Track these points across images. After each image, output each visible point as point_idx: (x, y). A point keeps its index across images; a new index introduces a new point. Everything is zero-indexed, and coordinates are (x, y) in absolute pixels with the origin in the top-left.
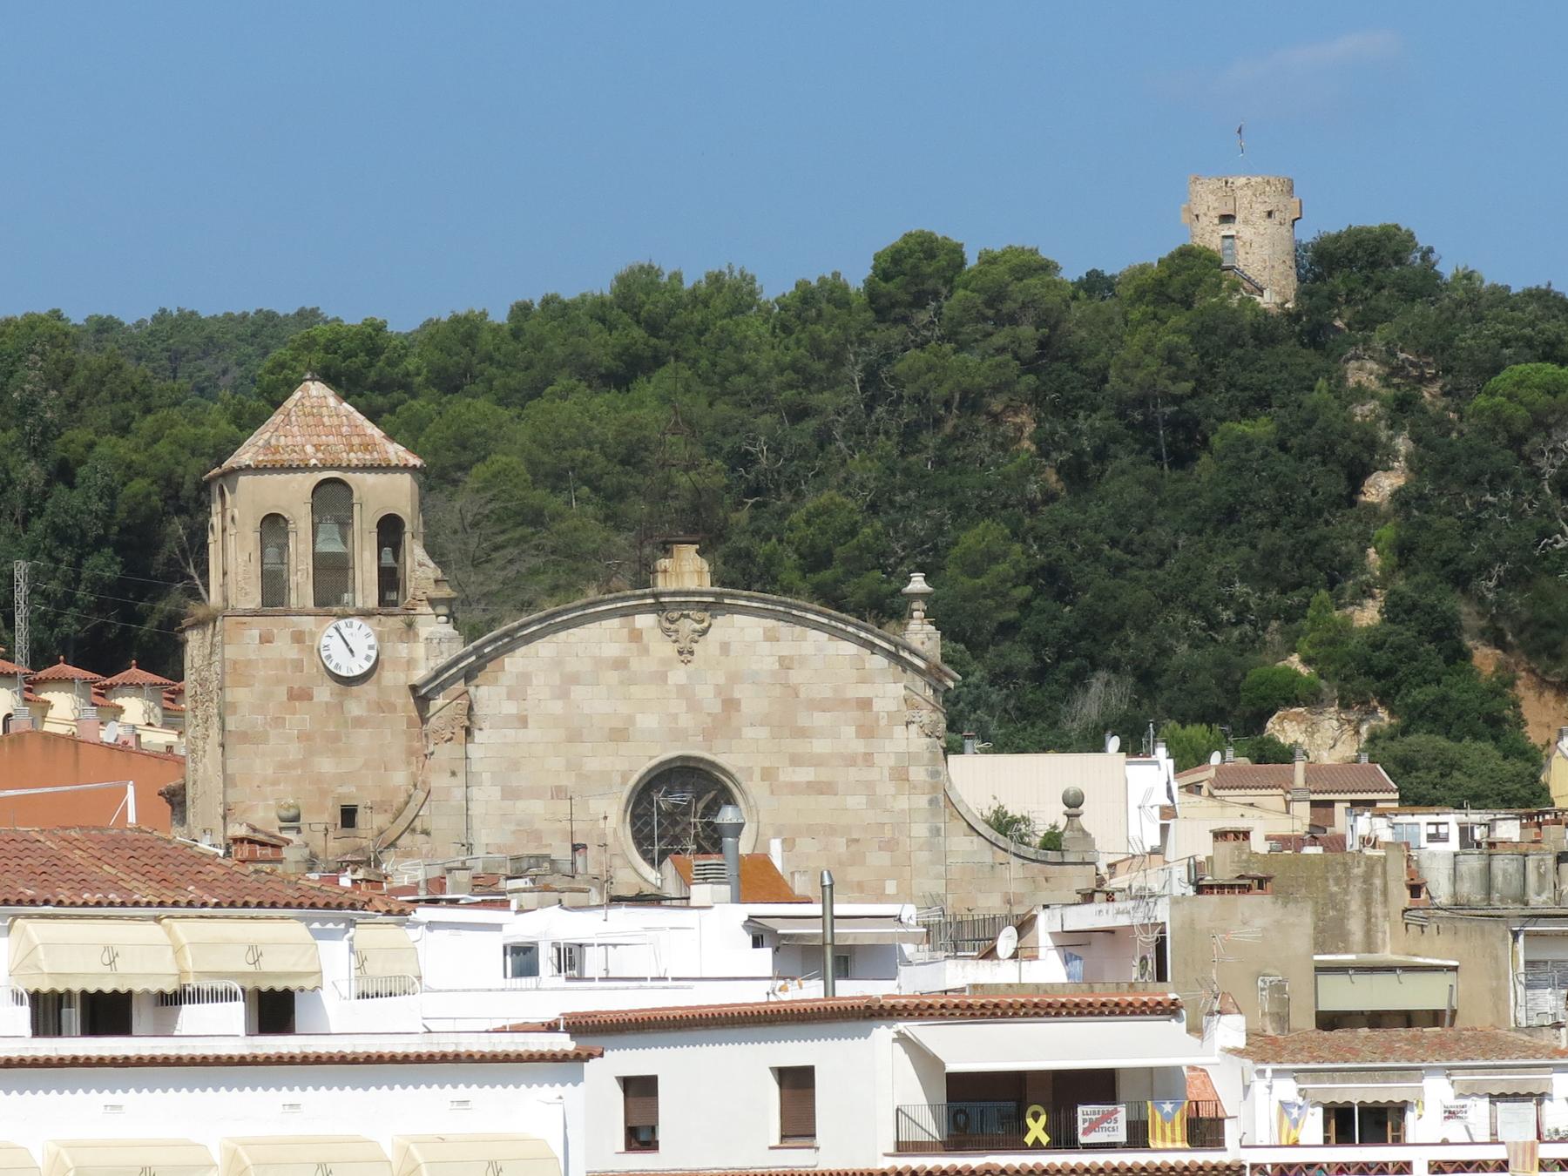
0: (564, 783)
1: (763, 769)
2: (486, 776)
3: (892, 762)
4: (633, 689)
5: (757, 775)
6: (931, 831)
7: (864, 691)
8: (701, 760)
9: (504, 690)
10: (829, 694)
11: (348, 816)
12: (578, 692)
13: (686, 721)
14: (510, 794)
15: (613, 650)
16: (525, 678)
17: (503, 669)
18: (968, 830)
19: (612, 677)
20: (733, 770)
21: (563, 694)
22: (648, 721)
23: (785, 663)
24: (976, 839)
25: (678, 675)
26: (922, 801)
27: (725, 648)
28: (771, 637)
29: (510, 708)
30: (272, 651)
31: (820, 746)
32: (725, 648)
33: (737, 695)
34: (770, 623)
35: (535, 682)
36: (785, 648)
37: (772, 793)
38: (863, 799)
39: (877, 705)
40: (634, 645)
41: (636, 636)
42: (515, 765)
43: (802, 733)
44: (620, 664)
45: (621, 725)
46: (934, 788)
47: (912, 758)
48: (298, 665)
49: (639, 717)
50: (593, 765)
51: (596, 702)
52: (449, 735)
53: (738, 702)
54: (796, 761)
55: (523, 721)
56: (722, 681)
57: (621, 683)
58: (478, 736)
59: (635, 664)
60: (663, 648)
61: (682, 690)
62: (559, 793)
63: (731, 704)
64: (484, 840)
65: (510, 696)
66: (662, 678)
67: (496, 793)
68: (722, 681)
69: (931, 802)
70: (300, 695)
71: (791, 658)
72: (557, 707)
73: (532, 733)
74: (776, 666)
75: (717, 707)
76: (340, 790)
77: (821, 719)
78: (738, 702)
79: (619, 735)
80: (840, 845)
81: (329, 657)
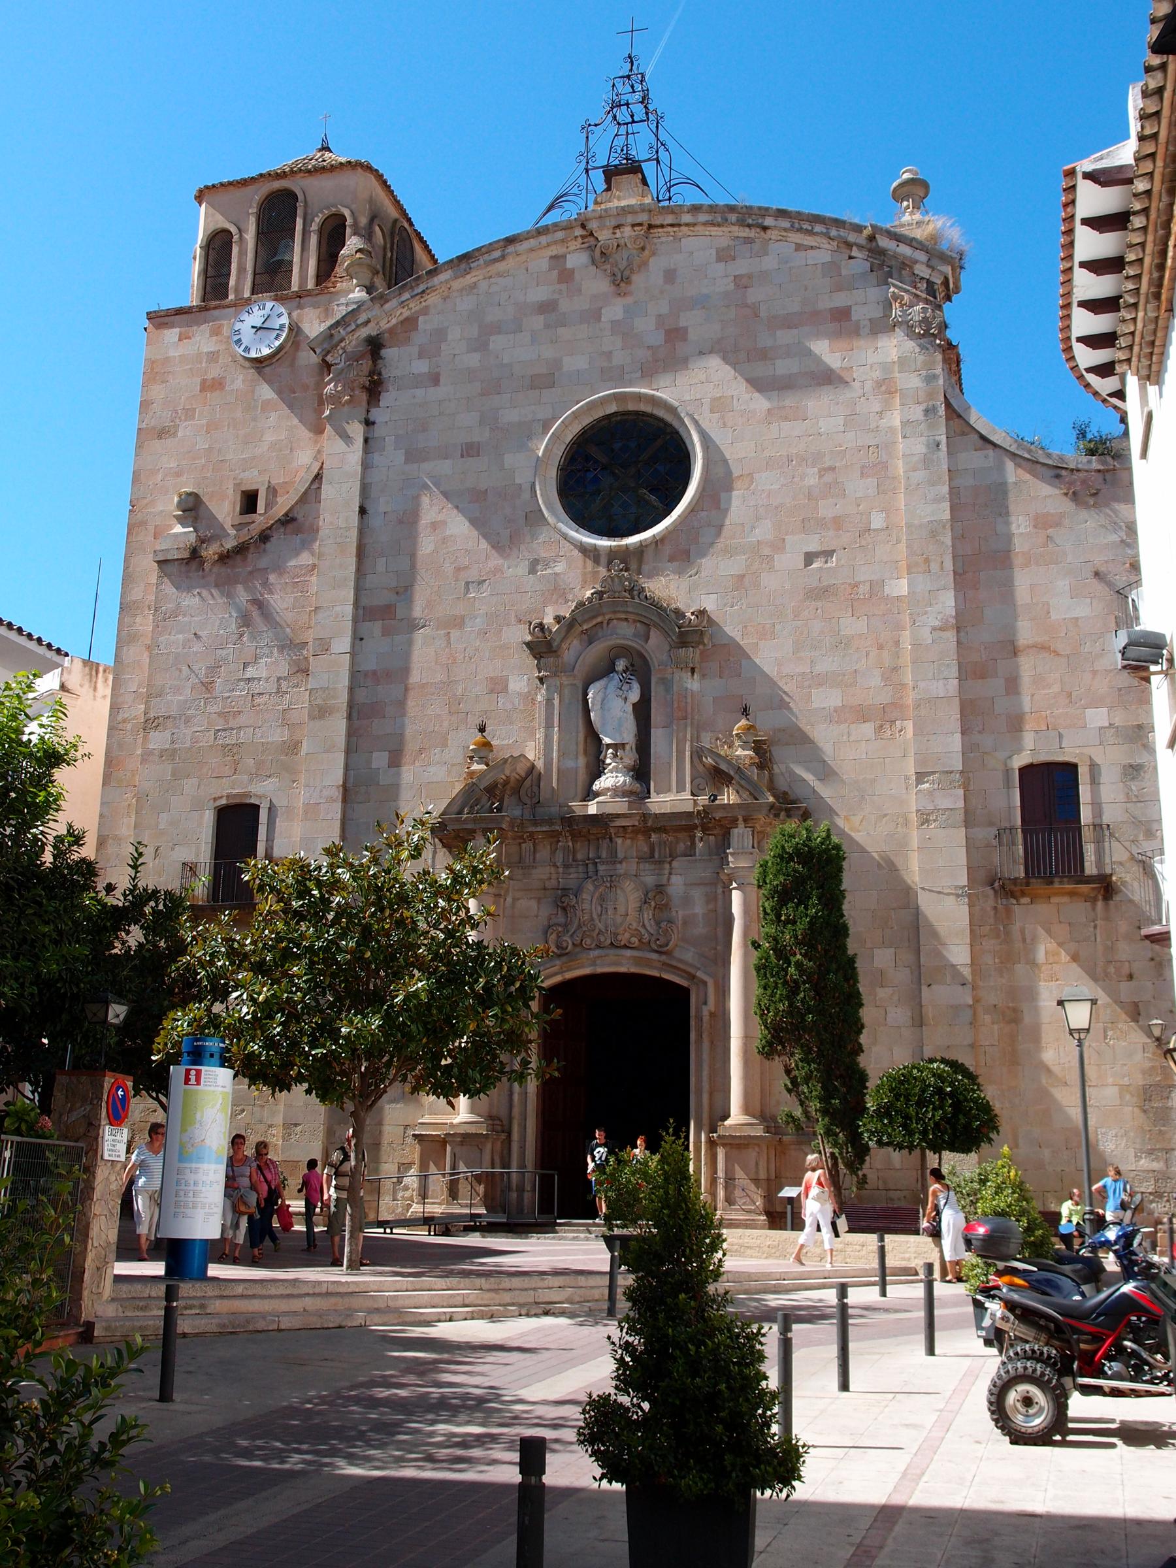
0: (476, 439)
1: (714, 400)
2: (390, 441)
3: (877, 374)
4: (561, 331)
5: (706, 407)
6: (928, 446)
7: (840, 300)
9: (415, 350)
11: (249, 501)
12: (497, 342)
13: (619, 358)
14: (414, 456)
15: (539, 294)
16: (440, 335)
18: (981, 442)
19: (538, 321)
20: (676, 404)
21: (480, 345)
22: (576, 363)
23: (742, 283)
24: (991, 452)
25: (614, 311)
26: (917, 413)
27: (670, 276)
28: (724, 256)
29: (421, 367)
30: (188, 348)
32: (670, 276)
33: (682, 323)
35: (450, 337)
36: (742, 266)
38: (841, 421)
40: (564, 287)
41: (566, 276)
43: (764, 355)
44: (546, 307)
45: (545, 371)
46: (931, 396)
47: (902, 362)
48: (213, 357)
49: (566, 360)
50: (510, 416)
51: (518, 351)
53: (685, 329)
55: (435, 380)
56: (664, 309)
57: (547, 326)
58: (386, 399)
59: (564, 305)
60: (596, 284)
61: (621, 328)
62: (470, 450)
63: (675, 335)
64: (382, 509)
65: (420, 357)
66: (596, 315)
67: (400, 457)
68: (664, 309)
69: (927, 411)
70: (212, 386)
71: (750, 276)
72: (473, 360)
73: (443, 390)
74: (732, 286)
75: (657, 339)
76: (242, 475)
77: (785, 337)
78: (685, 329)
79: (544, 380)
81: (240, 340)
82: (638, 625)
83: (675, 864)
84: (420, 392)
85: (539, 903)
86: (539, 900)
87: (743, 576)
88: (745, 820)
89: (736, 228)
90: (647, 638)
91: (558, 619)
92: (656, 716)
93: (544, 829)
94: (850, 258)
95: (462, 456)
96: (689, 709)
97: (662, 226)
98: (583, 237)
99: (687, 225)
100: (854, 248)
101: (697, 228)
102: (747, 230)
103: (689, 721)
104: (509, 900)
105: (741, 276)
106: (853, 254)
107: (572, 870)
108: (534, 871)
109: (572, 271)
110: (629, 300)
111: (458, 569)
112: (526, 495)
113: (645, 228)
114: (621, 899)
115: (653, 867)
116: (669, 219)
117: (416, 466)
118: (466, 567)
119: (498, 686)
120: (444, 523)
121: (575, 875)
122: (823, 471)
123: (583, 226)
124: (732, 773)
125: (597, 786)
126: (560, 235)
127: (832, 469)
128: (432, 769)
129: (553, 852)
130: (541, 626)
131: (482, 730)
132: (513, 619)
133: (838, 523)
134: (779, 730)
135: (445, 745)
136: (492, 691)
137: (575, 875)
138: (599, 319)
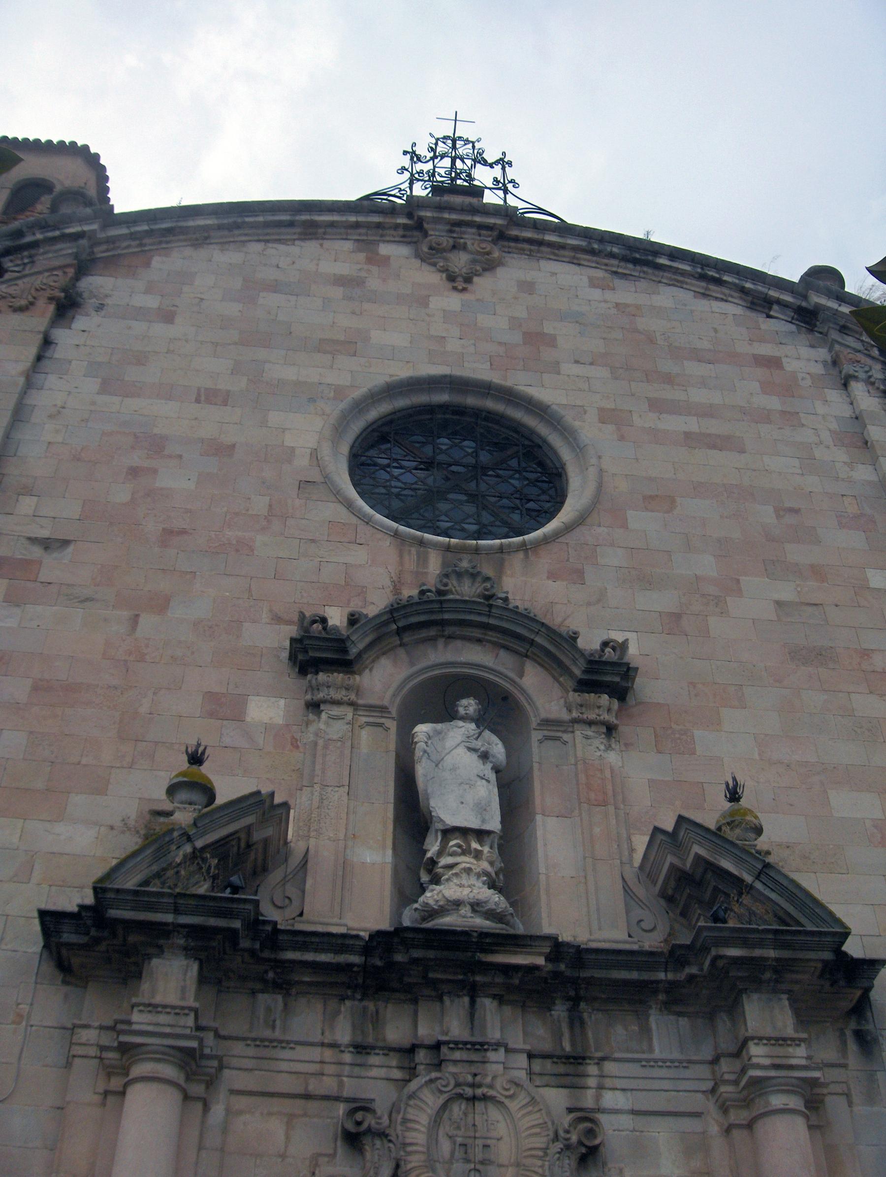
1: (601, 410)
4: (366, 306)
8: (486, 389)
10: (705, 344)
17: (148, 265)
31: (698, 396)
34: (599, 274)
37: (622, 438)
39: (791, 365)
42: (141, 359)
43: (669, 379)
52: (23, 302)
54: (657, 406)
55: (168, 317)
59: (374, 283)
67: (91, 385)
71: (638, 307)
77: (694, 369)
80: (766, 514)
82: (502, 653)
83: (610, 1067)
84: (139, 327)
85: (289, 1126)
86: (290, 1119)
87: (677, 617)
88: (776, 971)
89: (615, 262)
90: (521, 675)
91: (353, 619)
92: (544, 794)
93: (323, 958)
94: (769, 316)
95: (198, 401)
96: (609, 787)
97: (516, 239)
98: (405, 227)
99: (550, 244)
100: (775, 307)
101: (562, 252)
102: (631, 266)
103: (611, 808)
104: (218, 1111)
105: (627, 305)
106: (772, 313)
107: (374, 1060)
108: (287, 1054)
109: (387, 258)
110: (466, 296)
111: (169, 534)
112: (302, 461)
113: (495, 233)
114: (502, 1128)
115: (562, 1069)
116: (528, 234)
117: (116, 399)
118: (183, 532)
119: (225, 707)
120: (155, 471)
121: (382, 1073)
122: (781, 512)
123: (410, 215)
124: (748, 878)
125: (432, 896)
126: (376, 219)
127: (796, 511)
128: (61, 828)
129: (331, 1019)
130: (324, 620)
131: (196, 759)
132: (265, 617)
133: (818, 572)
134: (779, 845)
135: (100, 788)
136: (212, 715)
137: (382, 1073)
138: (426, 305)
